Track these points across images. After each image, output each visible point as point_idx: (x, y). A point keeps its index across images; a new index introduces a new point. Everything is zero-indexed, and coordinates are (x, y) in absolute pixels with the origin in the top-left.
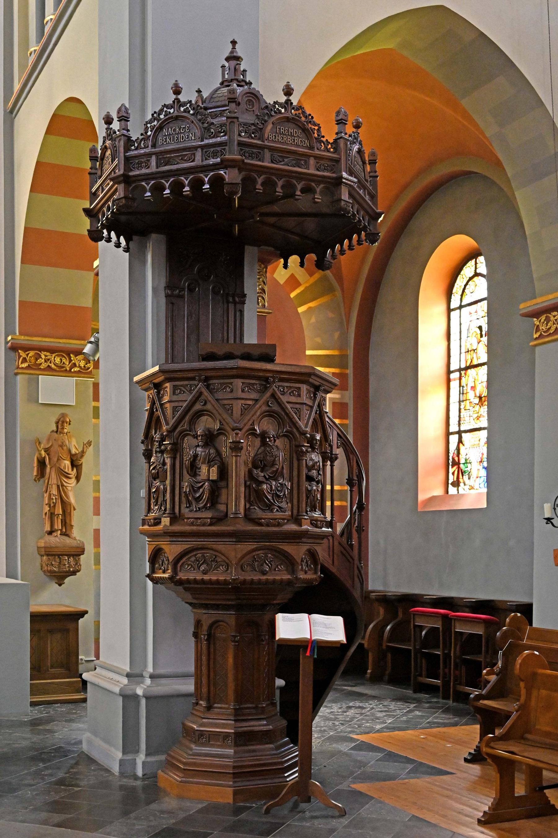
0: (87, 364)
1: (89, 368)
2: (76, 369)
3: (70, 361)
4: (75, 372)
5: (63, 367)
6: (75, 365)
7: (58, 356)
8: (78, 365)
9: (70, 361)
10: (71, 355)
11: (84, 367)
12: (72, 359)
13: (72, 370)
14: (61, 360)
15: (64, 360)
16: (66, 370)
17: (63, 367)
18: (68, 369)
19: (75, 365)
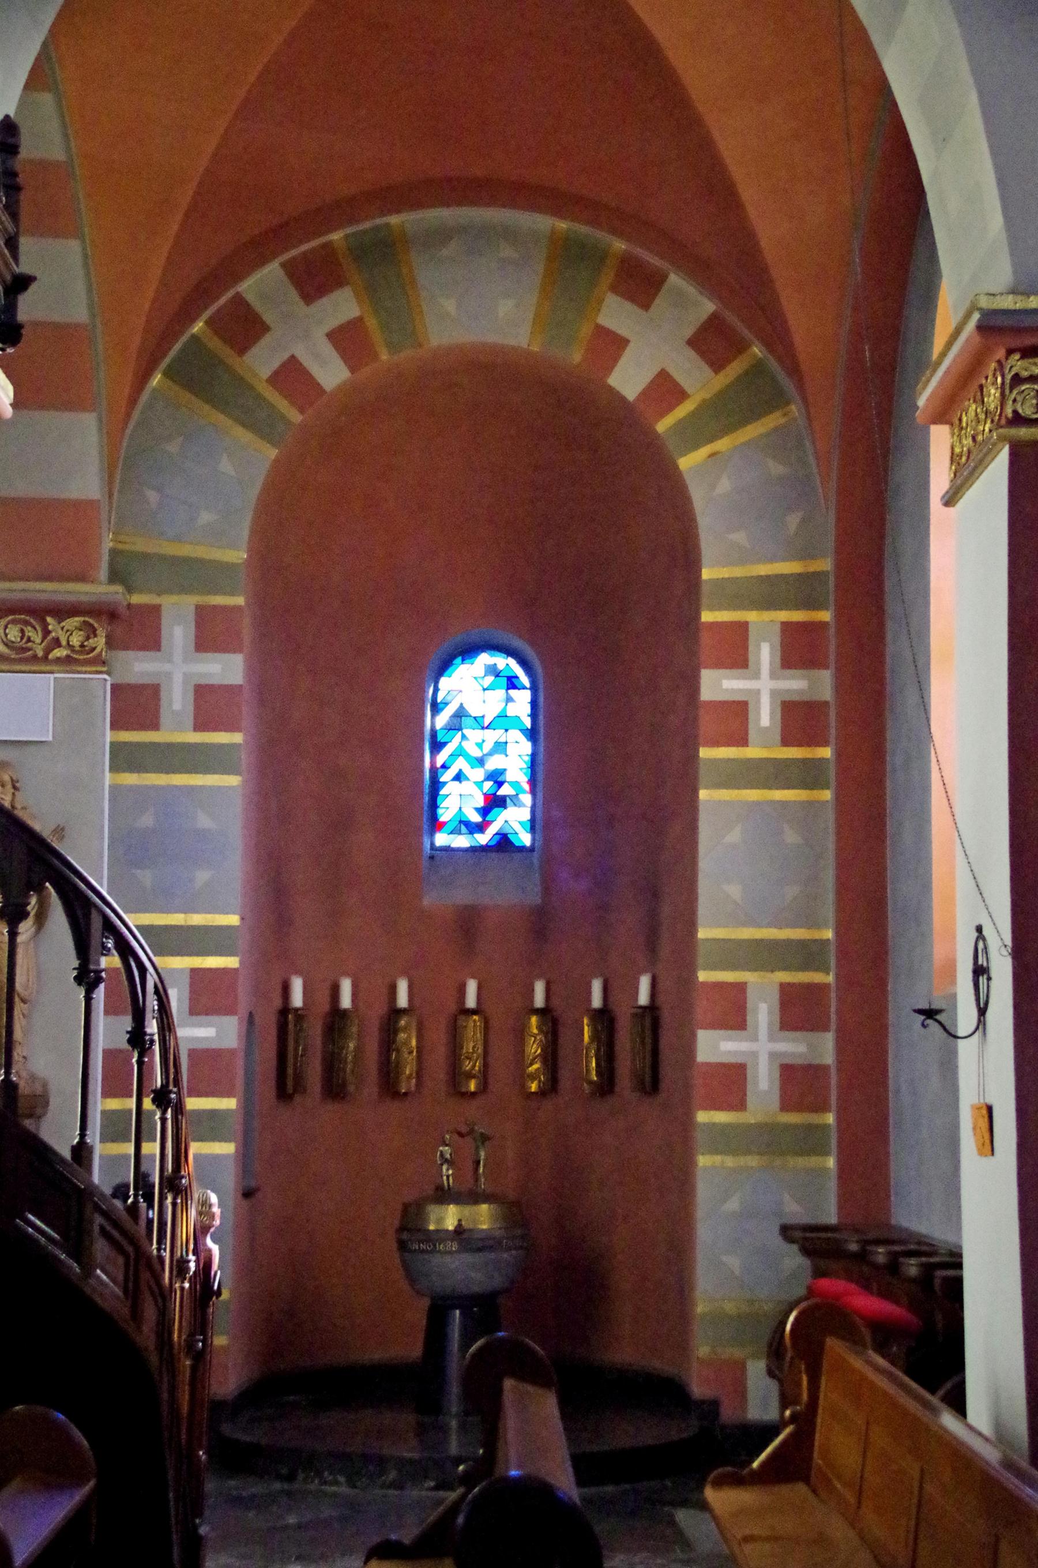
0: (88, 638)
1: (94, 649)
2: (58, 653)
3: (46, 632)
4: (58, 660)
5: (29, 649)
6: (57, 643)
7: (14, 622)
8: (64, 643)
9: (46, 632)
10: (49, 619)
11: (82, 646)
12: (50, 627)
13: (50, 656)
14: (22, 631)
15: (29, 632)
16: (35, 657)
17: (29, 649)
18: (40, 654)
19: (57, 643)
